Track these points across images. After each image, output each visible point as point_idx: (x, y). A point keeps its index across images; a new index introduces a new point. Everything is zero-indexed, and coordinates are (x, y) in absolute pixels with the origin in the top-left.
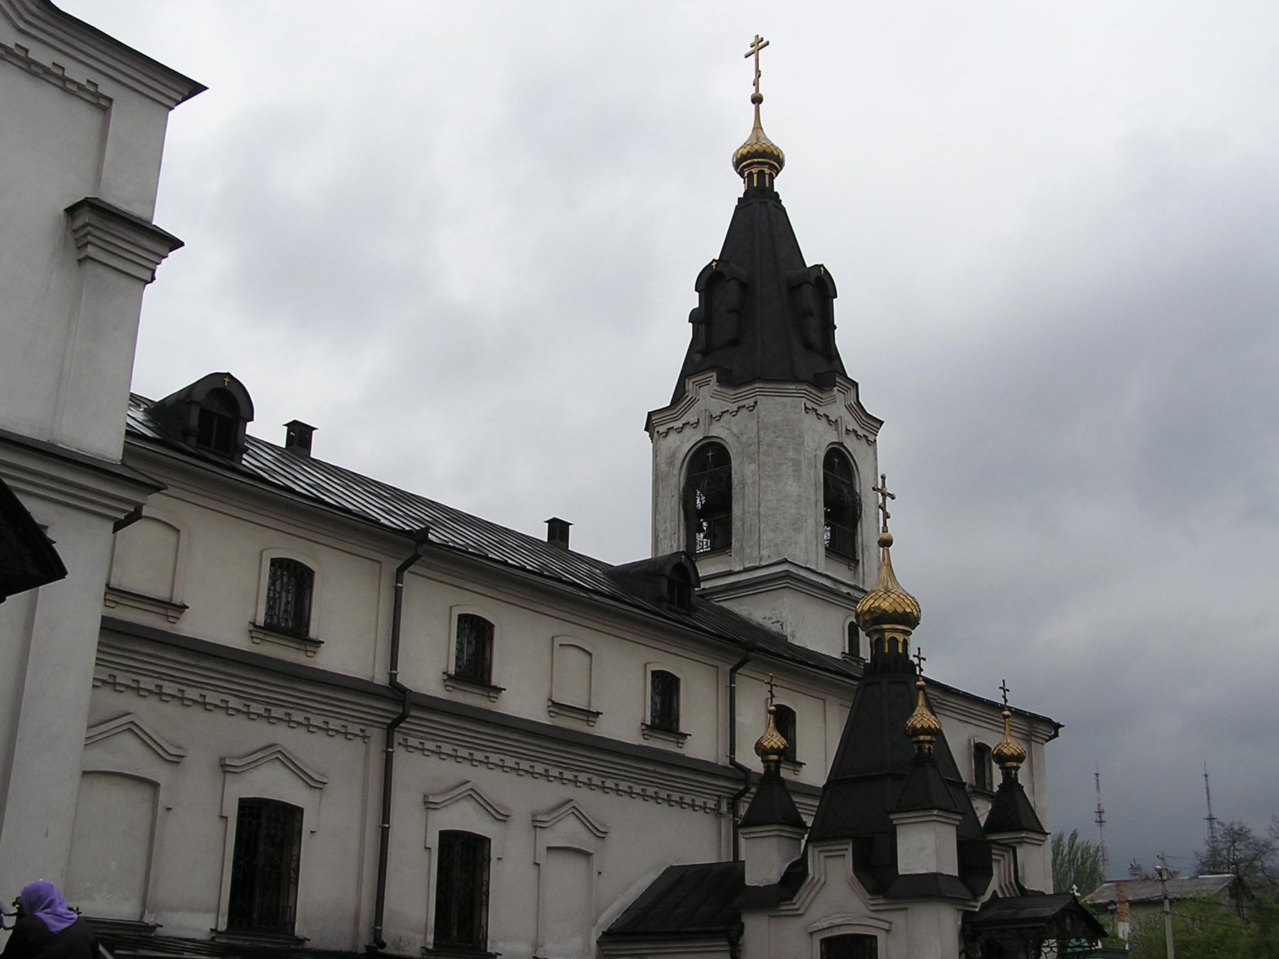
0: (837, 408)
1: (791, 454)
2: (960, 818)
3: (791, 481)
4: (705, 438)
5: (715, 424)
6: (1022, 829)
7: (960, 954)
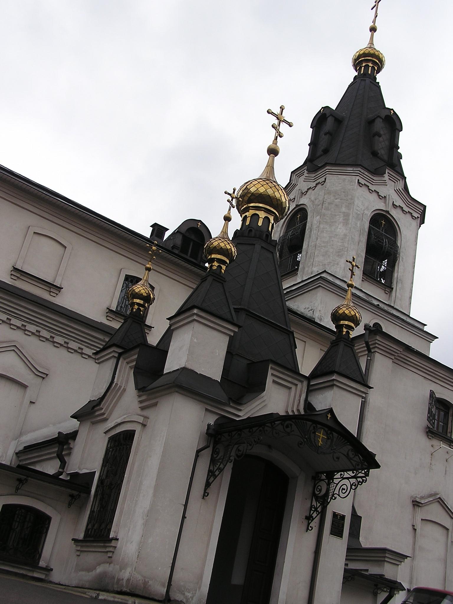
0: (389, 189)
1: (344, 209)
2: (236, 330)
3: (340, 226)
4: (297, 206)
5: (304, 197)
6: (332, 373)
7: (198, 452)
